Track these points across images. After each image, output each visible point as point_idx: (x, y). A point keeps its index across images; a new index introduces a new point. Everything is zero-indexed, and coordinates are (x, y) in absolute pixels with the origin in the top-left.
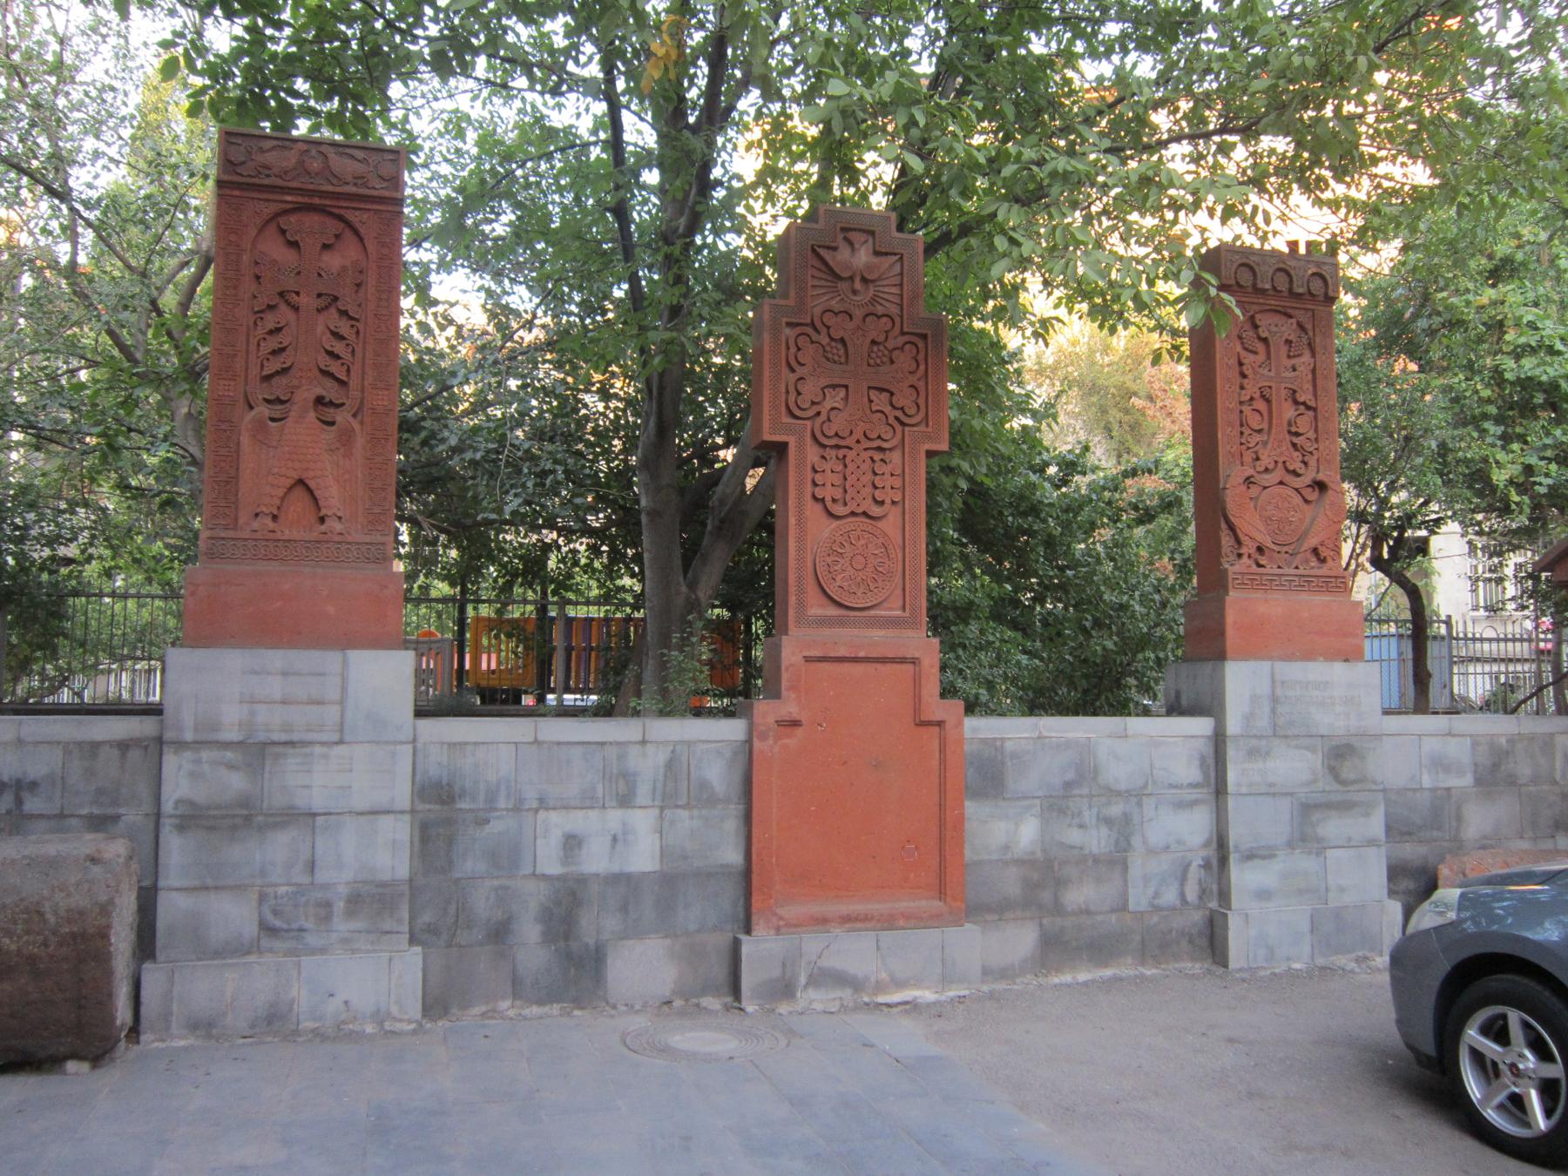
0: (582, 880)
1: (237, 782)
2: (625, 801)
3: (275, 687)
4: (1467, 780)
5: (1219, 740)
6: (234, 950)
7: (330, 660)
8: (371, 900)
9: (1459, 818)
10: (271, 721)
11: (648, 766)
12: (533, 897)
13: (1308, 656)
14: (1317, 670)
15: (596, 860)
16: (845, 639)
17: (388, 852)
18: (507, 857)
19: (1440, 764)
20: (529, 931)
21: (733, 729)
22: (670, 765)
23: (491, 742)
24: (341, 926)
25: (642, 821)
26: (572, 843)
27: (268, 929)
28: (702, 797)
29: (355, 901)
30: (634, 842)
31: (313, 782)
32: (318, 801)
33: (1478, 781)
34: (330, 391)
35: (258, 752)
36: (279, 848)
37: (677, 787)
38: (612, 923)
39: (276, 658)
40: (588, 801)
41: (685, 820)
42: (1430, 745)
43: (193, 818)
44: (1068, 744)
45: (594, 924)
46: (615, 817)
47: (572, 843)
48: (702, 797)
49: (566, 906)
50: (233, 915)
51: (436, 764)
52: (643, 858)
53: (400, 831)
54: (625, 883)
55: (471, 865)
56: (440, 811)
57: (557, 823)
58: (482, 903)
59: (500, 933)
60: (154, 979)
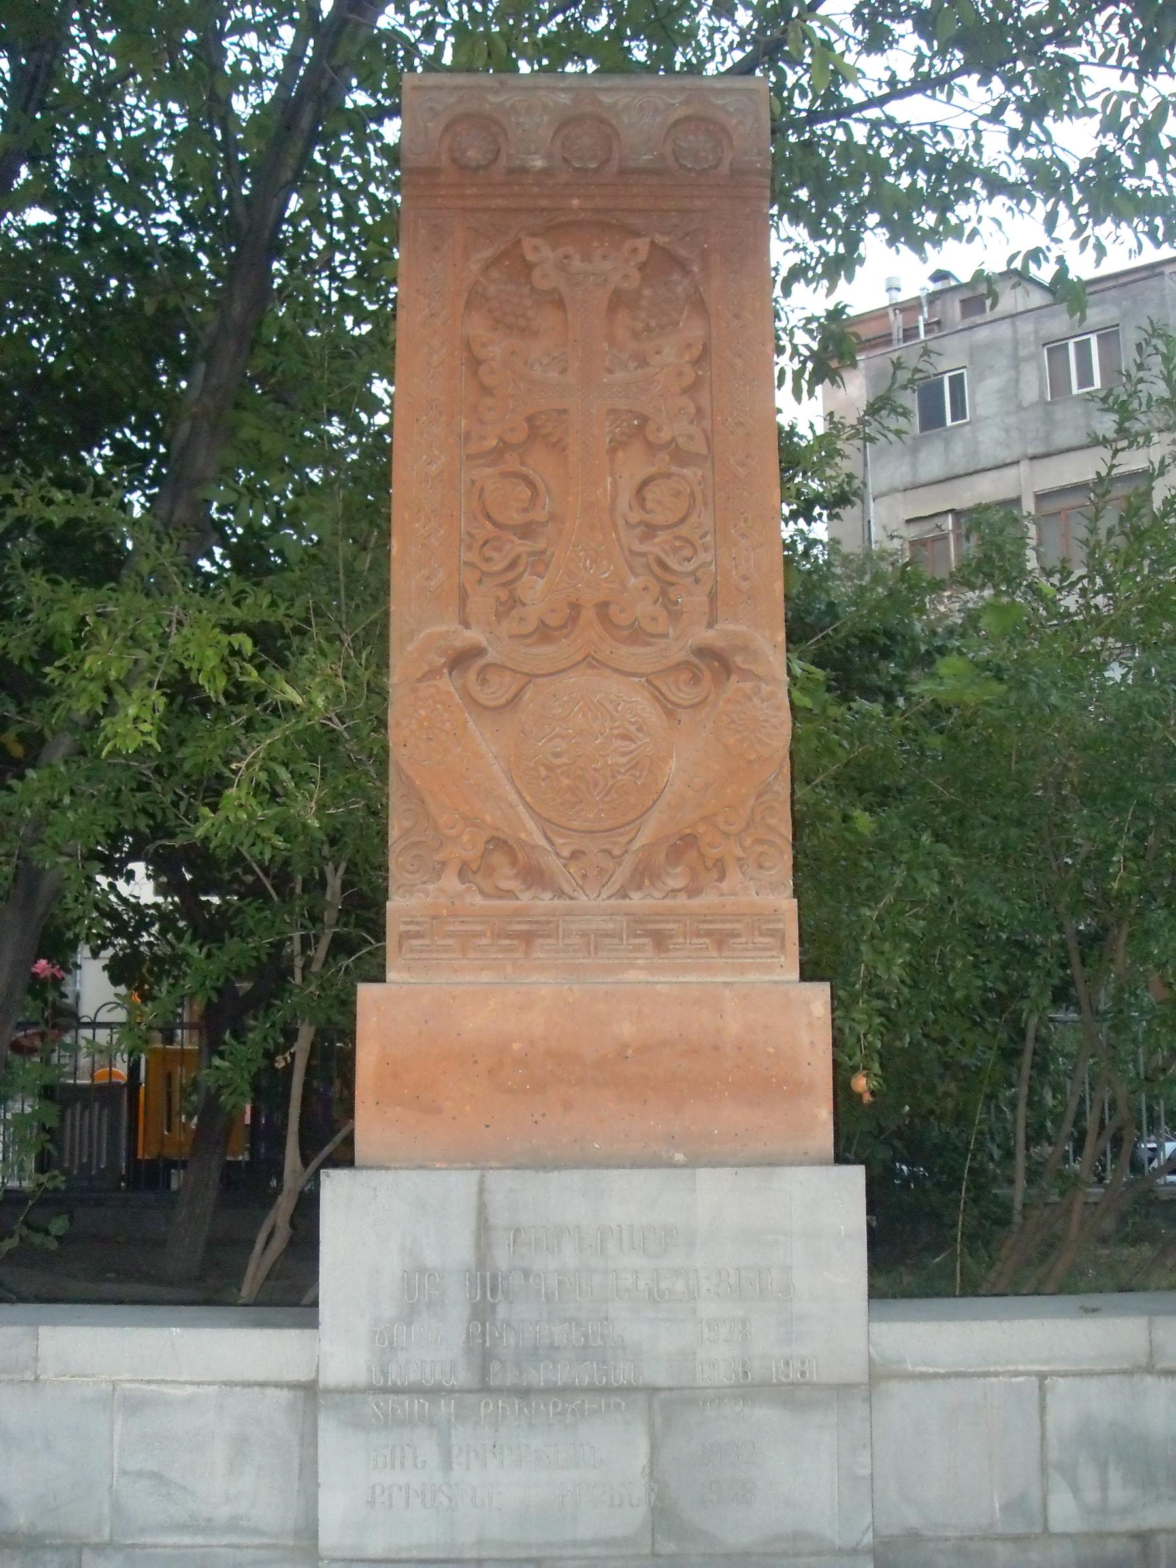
14: (628, 1199)
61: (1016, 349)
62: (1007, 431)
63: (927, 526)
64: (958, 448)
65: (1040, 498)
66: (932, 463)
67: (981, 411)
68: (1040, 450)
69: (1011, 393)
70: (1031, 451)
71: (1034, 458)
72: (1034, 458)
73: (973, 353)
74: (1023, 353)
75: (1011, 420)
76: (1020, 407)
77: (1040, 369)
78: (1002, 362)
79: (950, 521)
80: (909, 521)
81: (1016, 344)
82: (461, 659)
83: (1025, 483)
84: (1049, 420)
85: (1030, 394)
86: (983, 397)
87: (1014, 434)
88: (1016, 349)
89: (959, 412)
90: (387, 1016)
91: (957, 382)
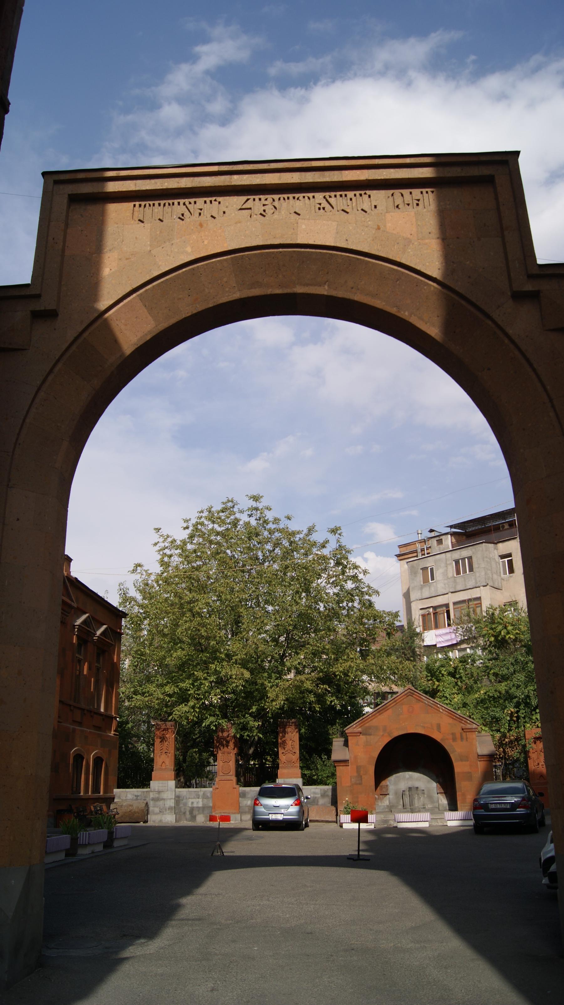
0: (194, 807)
1: (157, 795)
2: (198, 798)
3: (161, 785)
4: (320, 795)
5: (334, 791)
6: (157, 814)
7: (166, 782)
8: (170, 808)
9: (318, 801)
10: (161, 789)
11: (201, 794)
12: (188, 809)
13: (291, 778)
15: (195, 805)
16: (224, 778)
17: (171, 803)
18: (185, 804)
19: (314, 793)
20: (188, 813)
21: (211, 789)
22: (204, 794)
23: (184, 791)
24: (167, 811)
25: (200, 800)
26: (192, 803)
27: (160, 812)
28: (207, 798)
29: (169, 809)
30: (199, 803)
31: (164, 795)
32: (165, 798)
33: (321, 796)
34: (166, 751)
35: (159, 792)
36: (161, 803)
37: (205, 797)
38: (197, 813)
39: (161, 782)
40: (194, 798)
41: (205, 800)
42: (312, 790)
43: (153, 799)
44: (254, 791)
45: (195, 812)
46: (197, 800)
47: (192, 803)
48: (207, 798)
49: (192, 810)
50: (157, 810)
51: (177, 794)
52: (200, 805)
53: (173, 801)
54: (198, 808)
55: (181, 805)
56: (178, 799)
57: (191, 800)
58: (183, 810)
59: (185, 813)
60: (149, 816)
61: (446, 561)
62: (445, 585)
63: (426, 610)
64: (433, 589)
65: (455, 604)
66: (426, 594)
67: (438, 578)
68: (453, 591)
69: (445, 574)
70: (451, 591)
71: (452, 592)
72: (452, 592)
73: (436, 561)
74: (448, 562)
75: (446, 581)
76: (448, 578)
77: (453, 567)
78: (443, 565)
79: (431, 610)
80: (421, 609)
81: (446, 560)
82: (283, 753)
83: (451, 599)
84: (455, 582)
85: (450, 575)
86: (438, 574)
87: (447, 585)
88: (446, 561)
89: (433, 579)
90: (279, 772)
91: (432, 570)
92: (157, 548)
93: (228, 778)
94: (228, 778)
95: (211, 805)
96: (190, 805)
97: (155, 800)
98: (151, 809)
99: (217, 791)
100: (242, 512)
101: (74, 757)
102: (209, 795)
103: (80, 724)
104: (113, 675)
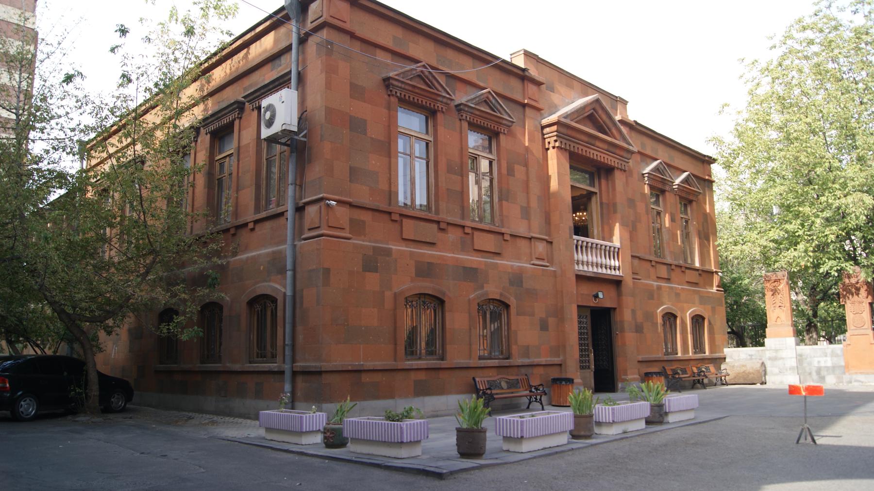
1: (774, 354)
8: (792, 368)
11: (829, 351)
15: (822, 364)
16: (856, 332)
17: (793, 362)
18: (810, 364)
20: (814, 374)
22: (832, 351)
23: (806, 349)
25: (829, 359)
26: (819, 362)
28: (837, 356)
30: (828, 362)
31: (783, 354)
35: (776, 351)
36: (780, 362)
37: (834, 354)
39: (777, 339)
43: (770, 359)
45: (823, 373)
47: (819, 362)
48: (837, 356)
49: (819, 371)
50: (776, 370)
51: (799, 352)
52: (829, 364)
54: (827, 368)
55: (805, 365)
56: (800, 358)
57: (816, 359)
59: (810, 374)
92: (743, 80)
93: (862, 332)
94: (862, 332)
95: (843, 364)
96: (816, 364)
97: (774, 359)
98: (768, 369)
99: (849, 347)
100: (842, 10)
101: (663, 317)
102: (839, 352)
103: (668, 280)
104: (707, 229)
